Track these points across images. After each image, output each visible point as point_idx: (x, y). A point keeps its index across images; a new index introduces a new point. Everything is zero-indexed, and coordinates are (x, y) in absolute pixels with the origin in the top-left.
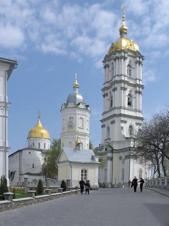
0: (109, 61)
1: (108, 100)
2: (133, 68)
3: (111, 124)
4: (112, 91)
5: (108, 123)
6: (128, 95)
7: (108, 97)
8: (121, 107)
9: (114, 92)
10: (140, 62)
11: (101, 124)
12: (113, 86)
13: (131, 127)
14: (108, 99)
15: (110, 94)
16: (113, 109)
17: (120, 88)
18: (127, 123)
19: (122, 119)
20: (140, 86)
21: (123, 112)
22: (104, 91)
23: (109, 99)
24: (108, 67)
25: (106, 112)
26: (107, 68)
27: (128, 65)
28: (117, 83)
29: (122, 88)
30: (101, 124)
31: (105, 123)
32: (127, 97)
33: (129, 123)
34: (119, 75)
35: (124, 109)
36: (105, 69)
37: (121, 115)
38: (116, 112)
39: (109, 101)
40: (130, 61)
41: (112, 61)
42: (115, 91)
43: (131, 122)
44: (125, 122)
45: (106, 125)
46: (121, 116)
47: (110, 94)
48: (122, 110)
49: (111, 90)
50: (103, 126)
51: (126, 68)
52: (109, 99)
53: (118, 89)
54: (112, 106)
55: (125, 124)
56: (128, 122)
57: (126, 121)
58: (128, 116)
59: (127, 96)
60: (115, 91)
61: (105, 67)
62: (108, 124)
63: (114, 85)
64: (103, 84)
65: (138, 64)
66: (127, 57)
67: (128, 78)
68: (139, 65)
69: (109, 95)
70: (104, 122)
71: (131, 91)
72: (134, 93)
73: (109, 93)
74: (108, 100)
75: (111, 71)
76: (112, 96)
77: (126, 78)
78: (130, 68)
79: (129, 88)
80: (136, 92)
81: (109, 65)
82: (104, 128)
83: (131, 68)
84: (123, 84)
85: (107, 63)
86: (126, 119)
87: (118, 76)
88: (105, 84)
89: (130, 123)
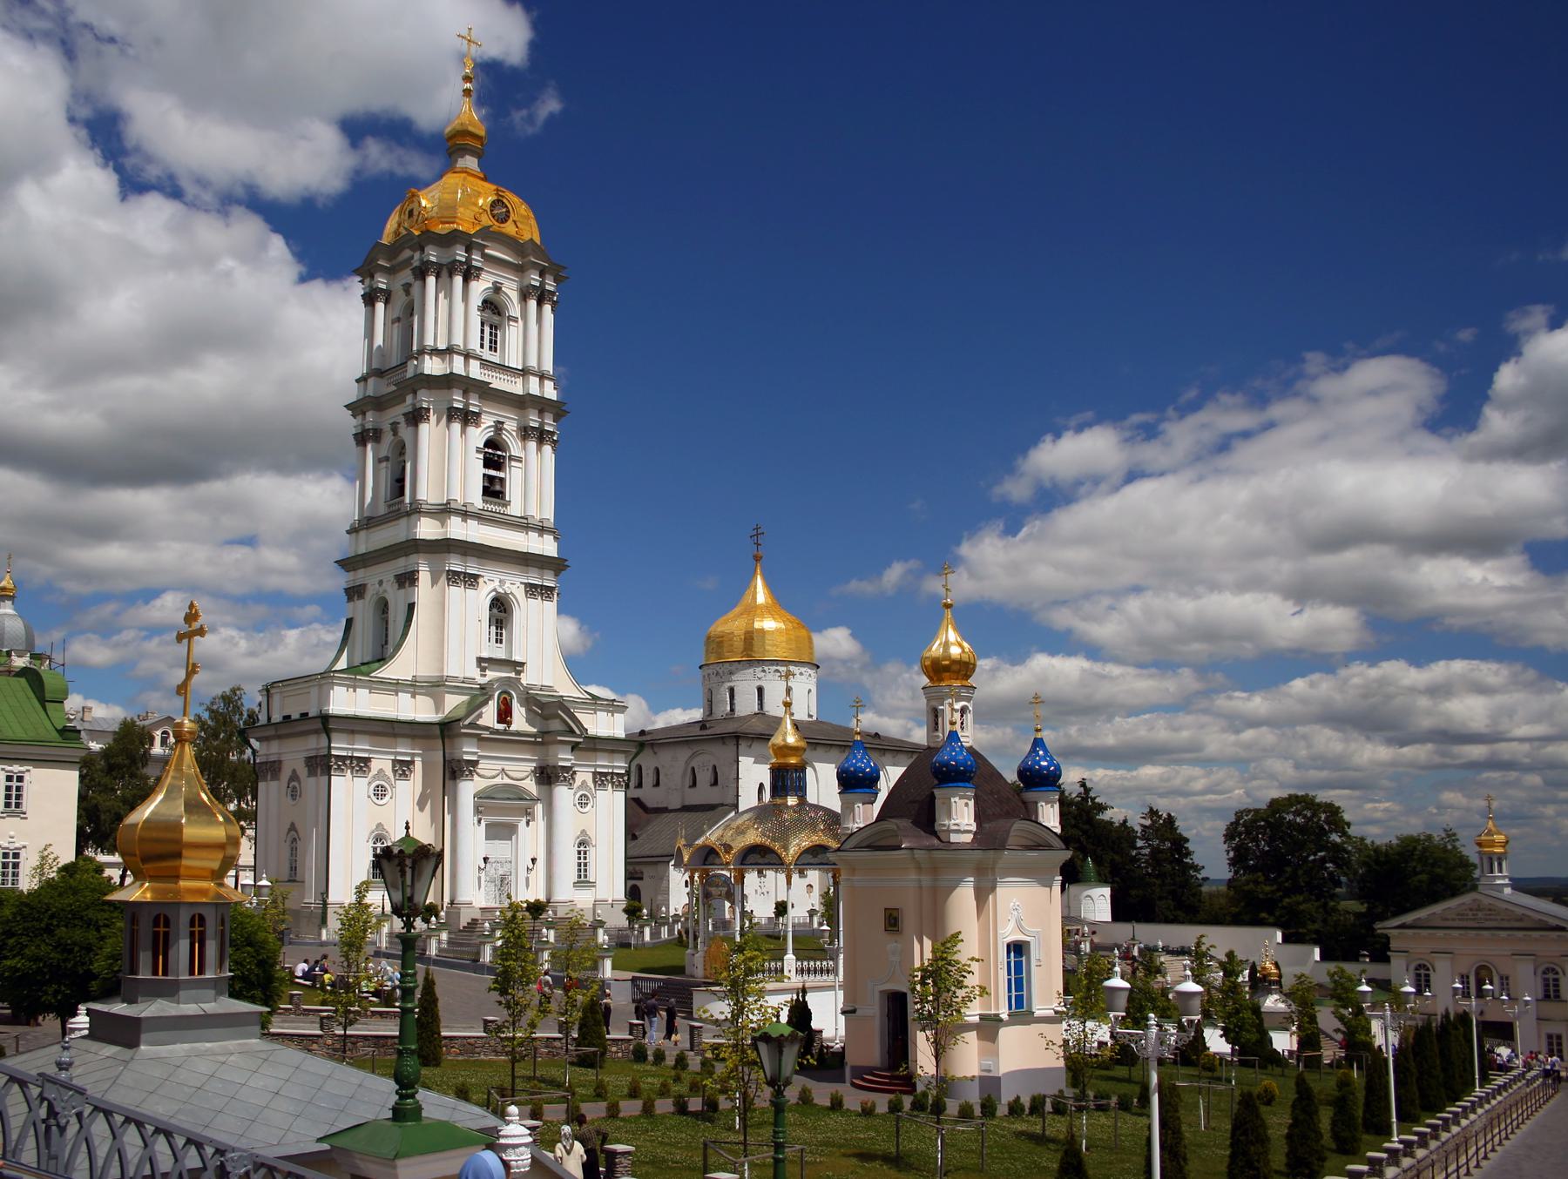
2: (510, 318)
4: (402, 420)
5: (379, 578)
8: (448, 503)
9: (411, 429)
12: (409, 399)
14: (383, 454)
16: (408, 514)
19: (456, 564)
20: (541, 404)
21: (458, 529)
22: (364, 414)
23: (387, 459)
25: (370, 519)
27: (485, 302)
28: (429, 388)
29: (452, 414)
30: (342, 580)
31: (361, 576)
33: (491, 586)
34: (442, 346)
35: (465, 514)
38: (427, 529)
41: (406, 276)
44: (471, 580)
49: (397, 413)
51: (476, 318)
52: (387, 459)
54: (402, 493)
57: (476, 577)
59: (478, 450)
62: (381, 583)
63: (415, 393)
64: (358, 381)
65: (533, 304)
66: (480, 269)
67: (486, 364)
68: (540, 304)
69: (388, 438)
70: (361, 573)
71: (499, 427)
73: (386, 427)
76: (404, 447)
77: (474, 365)
78: (496, 318)
80: (525, 433)
82: (359, 603)
87: (435, 352)
88: (362, 380)
89: (497, 583)
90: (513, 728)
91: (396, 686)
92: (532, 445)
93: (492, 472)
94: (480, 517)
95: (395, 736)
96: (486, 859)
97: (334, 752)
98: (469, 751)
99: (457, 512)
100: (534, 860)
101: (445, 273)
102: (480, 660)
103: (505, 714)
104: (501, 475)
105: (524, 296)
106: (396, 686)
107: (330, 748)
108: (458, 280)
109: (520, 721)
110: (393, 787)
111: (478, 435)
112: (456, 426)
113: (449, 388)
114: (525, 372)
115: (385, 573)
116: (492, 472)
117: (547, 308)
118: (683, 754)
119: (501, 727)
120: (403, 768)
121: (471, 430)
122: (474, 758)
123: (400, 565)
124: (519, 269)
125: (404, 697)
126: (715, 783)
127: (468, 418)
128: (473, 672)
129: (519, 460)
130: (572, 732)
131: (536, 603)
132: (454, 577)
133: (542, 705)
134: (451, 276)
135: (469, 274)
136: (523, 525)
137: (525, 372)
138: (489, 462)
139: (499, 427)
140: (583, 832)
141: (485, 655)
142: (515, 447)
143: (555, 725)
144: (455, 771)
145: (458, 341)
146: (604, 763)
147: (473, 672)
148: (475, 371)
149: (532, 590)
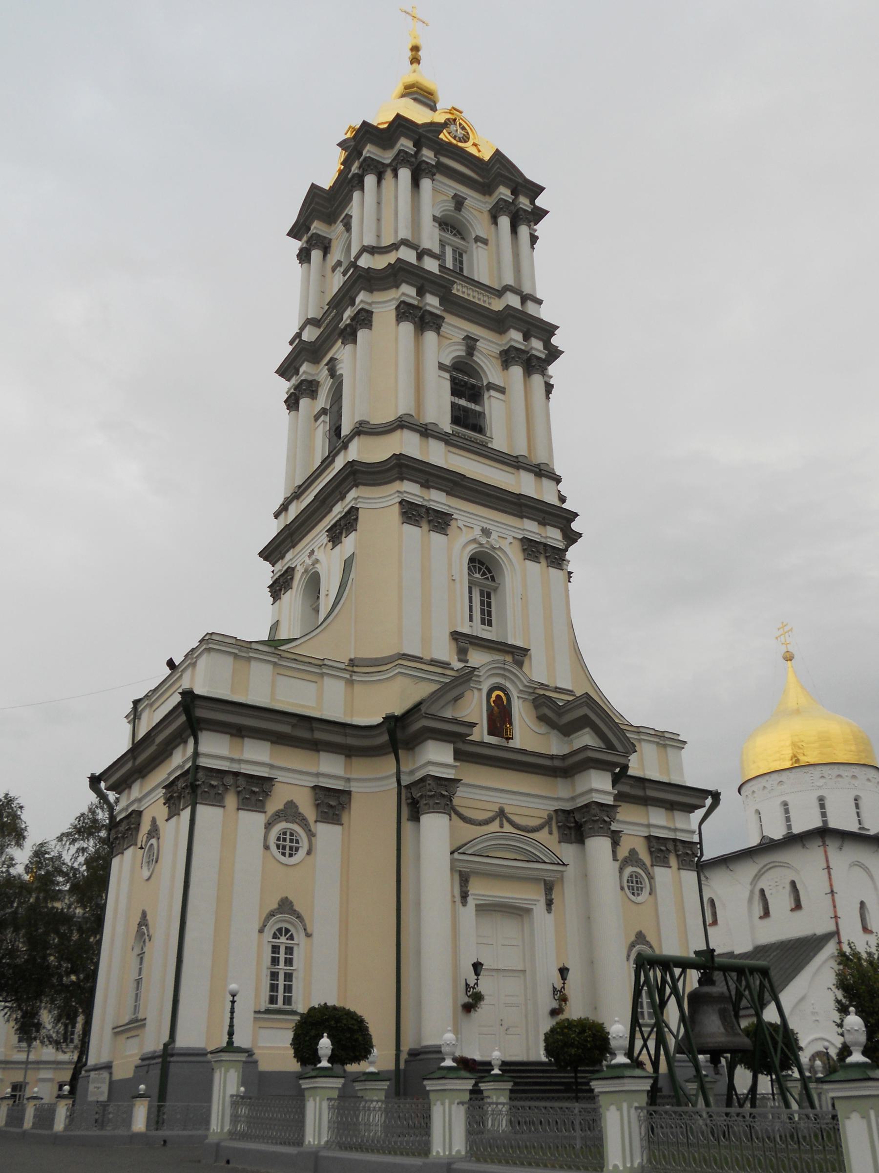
0: (330, 219)
1: (316, 418)
2: (478, 239)
3: (330, 545)
6: (447, 362)
7: (322, 400)
9: (349, 347)
10: (521, 212)
11: (266, 572)
13: (482, 563)
15: (332, 372)
17: (393, 315)
18: (450, 531)
23: (324, 411)
24: (326, 250)
25: (300, 487)
26: (316, 254)
28: (371, 291)
32: (447, 376)
34: (386, 242)
36: (305, 265)
37: (403, 467)
39: (322, 418)
40: (459, 202)
42: (362, 334)
44: (440, 522)
45: (298, 567)
46: (402, 479)
47: (332, 372)
50: (279, 587)
53: (375, 319)
55: (436, 538)
56: (460, 524)
58: (456, 483)
59: (442, 367)
60: (355, 341)
61: (304, 256)
63: (353, 303)
65: (504, 222)
68: (514, 230)
70: (289, 556)
71: (470, 343)
72: (497, 363)
74: (316, 418)
75: (339, 263)
80: (508, 357)
81: (330, 240)
82: (287, 597)
83: (463, 239)
84: (408, 292)
85: (317, 227)
86: (437, 499)
88: (298, 335)
89: (477, 532)
91: (320, 668)
92: (517, 371)
93: (463, 402)
94: (446, 439)
95: (317, 747)
96: (477, 967)
97: (203, 762)
98: (437, 757)
100: (563, 972)
101: (389, 174)
102: (456, 636)
103: (500, 718)
104: (478, 408)
105: (494, 220)
106: (320, 668)
107: (196, 754)
108: (405, 174)
109: (527, 733)
110: (311, 834)
111: (441, 348)
112: (407, 328)
113: (397, 287)
114: (499, 293)
115: (319, 535)
116: (463, 402)
117: (524, 231)
118: (747, 871)
119: (493, 740)
120: (332, 803)
121: (430, 337)
122: (449, 774)
123: (338, 510)
124: (486, 189)
126: (798, 906)
127: (424, 321)
128: (445, 651)
129: (502, 390)
130: (610, 746)
131: (535, 569)
132: (412, 513)
133: (561, 711)
134: (396, 176)
136: (515, 463)
137: (499, 293)
139: (470, 343)
140: (640, 937)
141: (466, 630)
142: (492, 372)
143: (586, 738)
144: (421, 798)
145: (404, 233)
146: (659, 821)
147: (445, 651)
148: (431, 265)
149: (533, 549)
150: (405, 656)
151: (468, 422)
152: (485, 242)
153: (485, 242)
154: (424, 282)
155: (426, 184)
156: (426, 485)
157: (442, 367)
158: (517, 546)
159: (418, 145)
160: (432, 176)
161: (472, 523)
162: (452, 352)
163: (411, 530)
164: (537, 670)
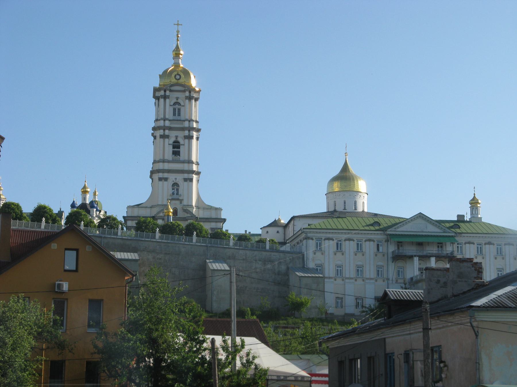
18: (169, 180)
19: (161, 175)
43: (176, 179)
44: (166, 179)
48: (161, 164)
55: (165, 183)
59: (169, 144)
65: (187, 101)
79: (173, 134)
80: (186, 137)
90: (178, 217)
99: (161, 162)
112: (162, 140)
116: (176, 150)
124: (184, 91)
125: (148, 210)
129: (184, 145)
132: (160, 179)
135: (165, 97)
136: (183, 162)
138: (174, 147)
149: (185, 180)
150: (158, 205)
151: (176, 153)
152: (184, 106)
153: (184, 106)
154: (164, 128)
155: (167, 100)
156: (163, 173)
157: (169, 144)
158: (183, 181)
159: (165, 91)
160: (169, 98)
161: (172, 177)
162: (172, 140)
163: (161, 182)
164: (185, 202)
